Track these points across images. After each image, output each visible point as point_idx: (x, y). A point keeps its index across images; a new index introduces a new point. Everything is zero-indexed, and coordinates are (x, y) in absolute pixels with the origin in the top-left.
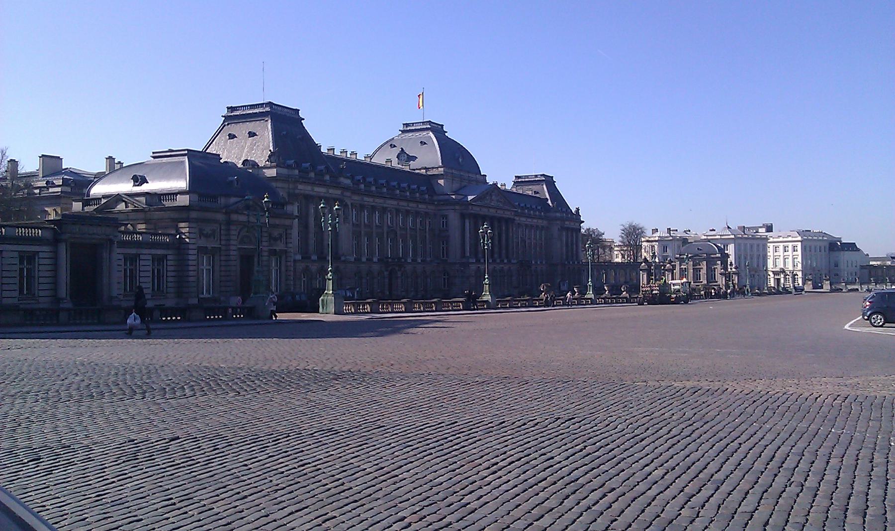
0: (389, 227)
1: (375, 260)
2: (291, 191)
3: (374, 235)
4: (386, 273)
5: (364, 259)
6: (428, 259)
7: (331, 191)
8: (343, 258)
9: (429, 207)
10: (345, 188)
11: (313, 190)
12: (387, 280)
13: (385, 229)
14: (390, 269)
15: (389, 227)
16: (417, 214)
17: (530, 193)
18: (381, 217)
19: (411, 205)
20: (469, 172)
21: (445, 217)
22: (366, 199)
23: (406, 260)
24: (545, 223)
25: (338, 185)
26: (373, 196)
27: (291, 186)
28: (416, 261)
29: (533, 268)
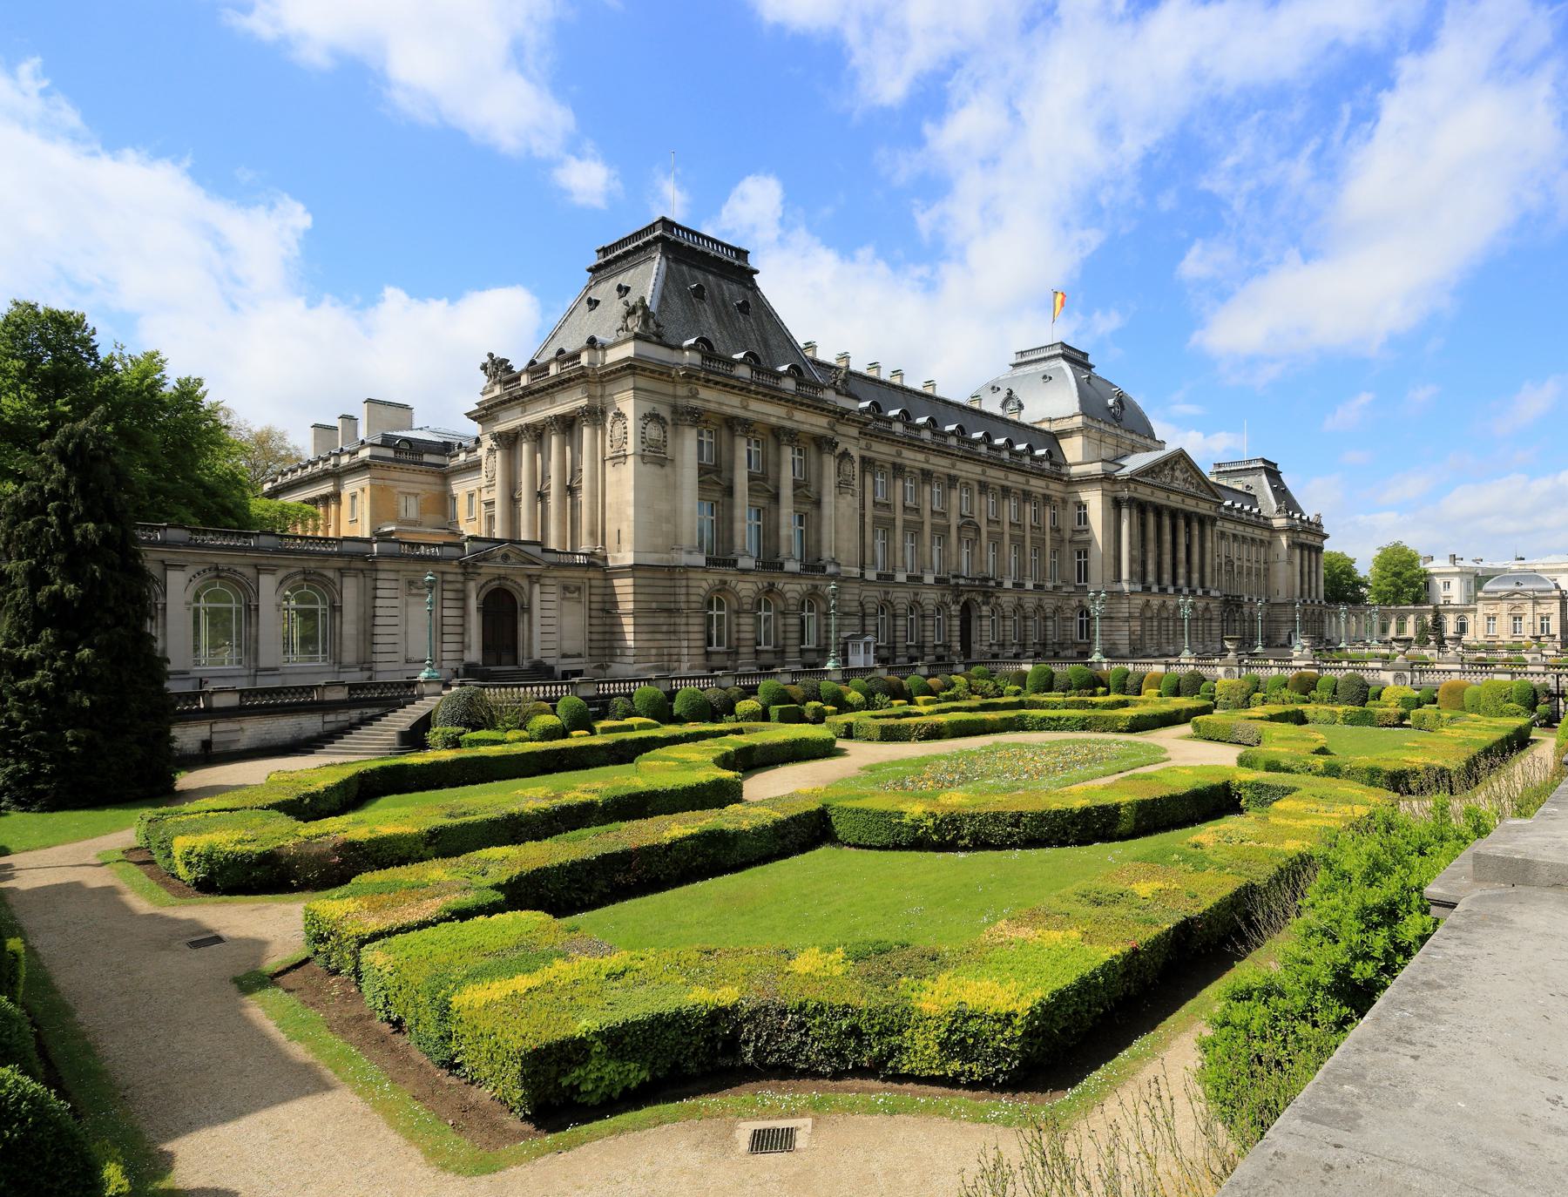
0: (962, 516)
1: (929, 579)
2: (683, 402)
3: (927, 528)
4: (955, 609)
5: (901, 577)
6: (1049, 585)
7: (799, 415)
8: (831, 569)
9: (1052, 486)
10: (842, 415)
11: (745, 408)
12: (956, 622)
13: (954, 521)
14: (962, 599)
15: (962, 516)
16: (1027, 496)
17: (1239, 487)
18: (945, 498)
19: (1013, 477)
20: (1132, 432)
21: (1082, 506)
22: (907, 453)
23: (1000, 584)
24: (1266, 535)
25: (819, 407)
26: (922, 448)
27: (682, 391)
28: (1023, 585)
29: (1246, 610)
